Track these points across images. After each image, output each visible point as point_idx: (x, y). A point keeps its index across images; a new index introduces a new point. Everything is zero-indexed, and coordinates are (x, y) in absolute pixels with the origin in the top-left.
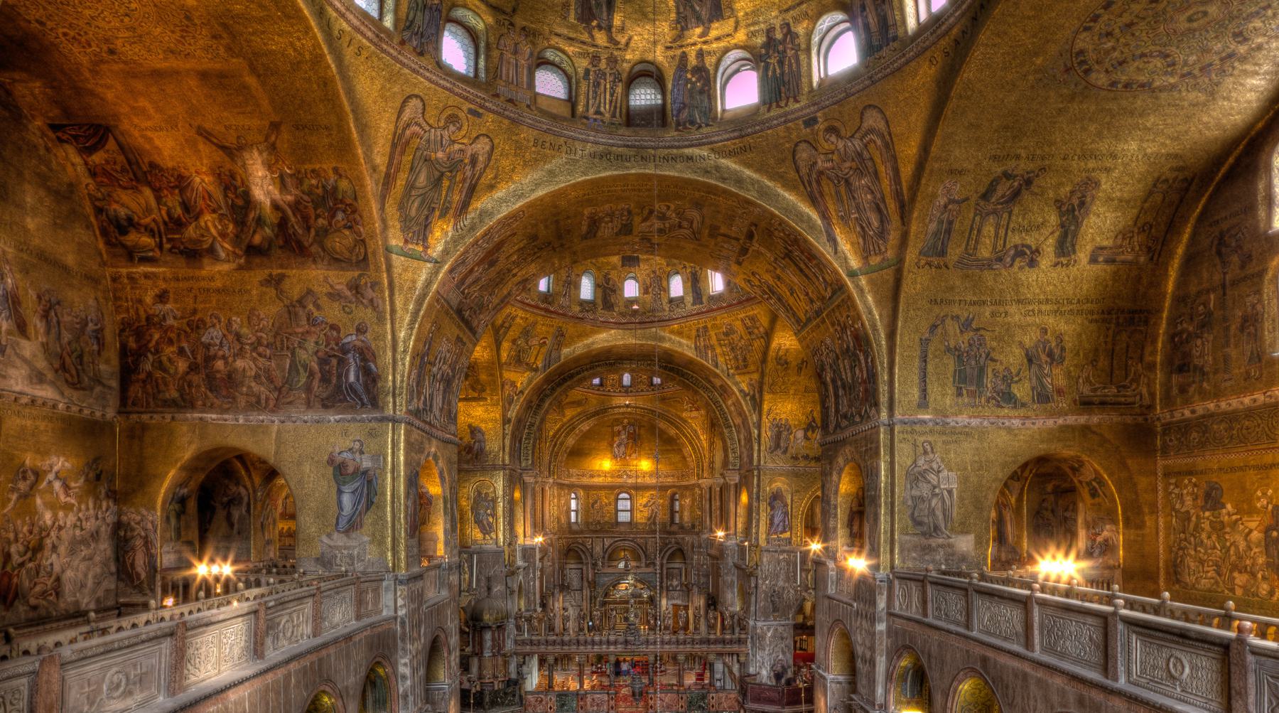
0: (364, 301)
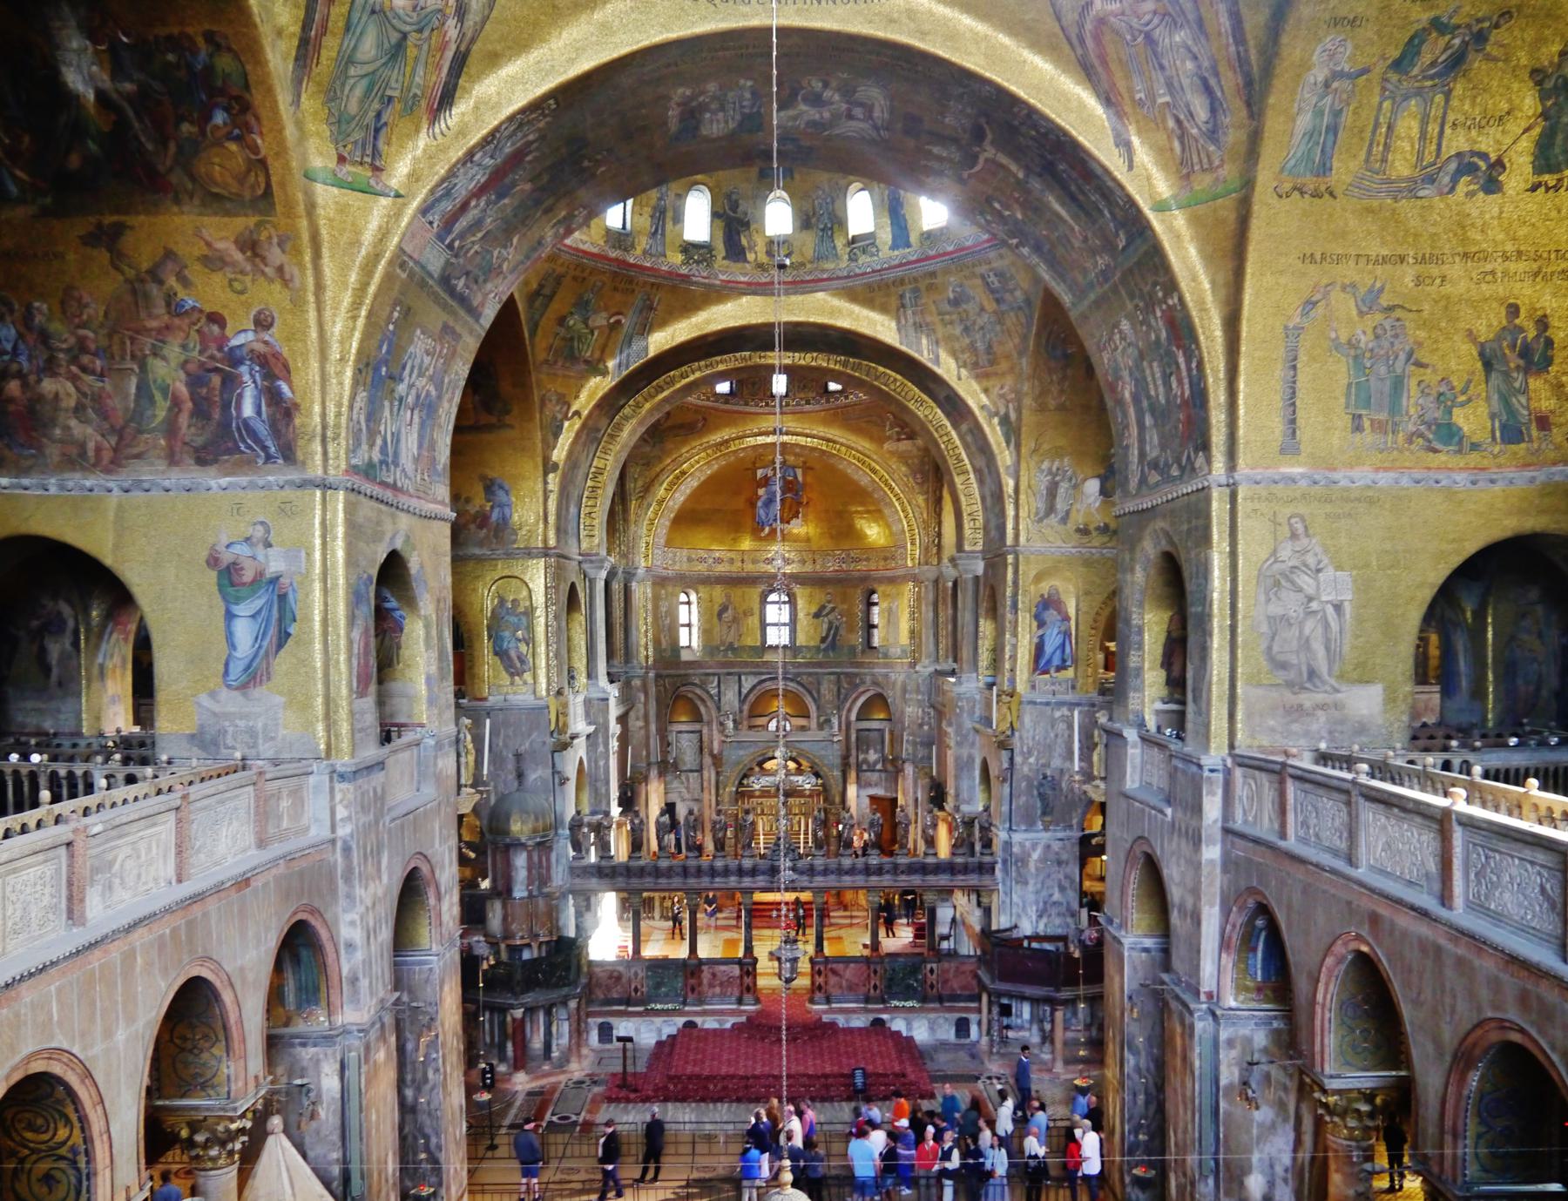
0: (267, 270)
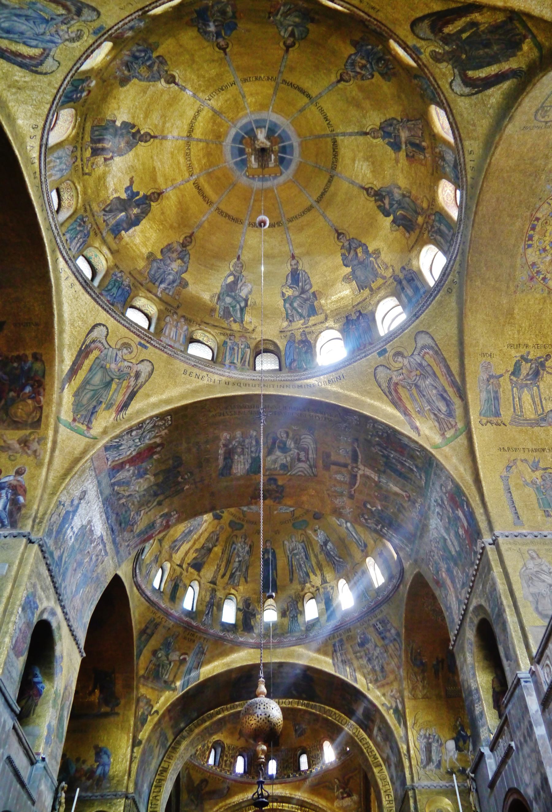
0: (29, 452)
